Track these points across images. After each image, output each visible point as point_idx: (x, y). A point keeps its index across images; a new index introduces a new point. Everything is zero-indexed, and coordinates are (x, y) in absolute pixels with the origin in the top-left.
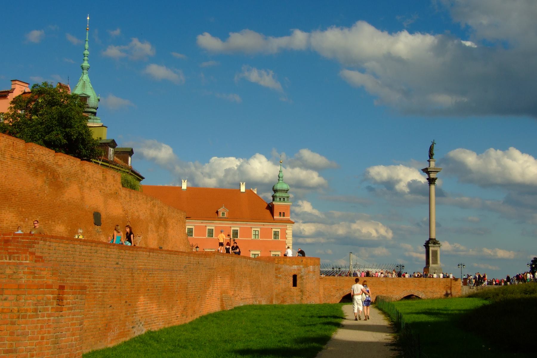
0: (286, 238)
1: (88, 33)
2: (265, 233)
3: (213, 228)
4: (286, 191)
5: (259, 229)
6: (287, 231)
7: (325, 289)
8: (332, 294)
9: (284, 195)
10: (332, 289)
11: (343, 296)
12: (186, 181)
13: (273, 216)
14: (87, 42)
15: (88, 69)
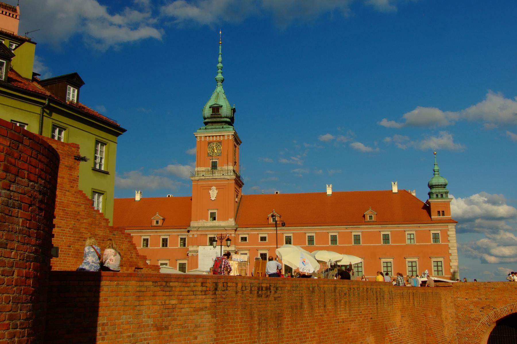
0: (449, 241)
1: (220, 47)
2: (422, 236)
3: (360, 234)
4: (445, 186)
5: (414, 232)
6: (449, 233)
7: (457, 307)
8: (473, 316)
9: (441, 190)
10: (472, 307)
11: (494, 320)
12: (331, 186)
13: (430, 216)
14: (220, 55)
15: (222, 81)
